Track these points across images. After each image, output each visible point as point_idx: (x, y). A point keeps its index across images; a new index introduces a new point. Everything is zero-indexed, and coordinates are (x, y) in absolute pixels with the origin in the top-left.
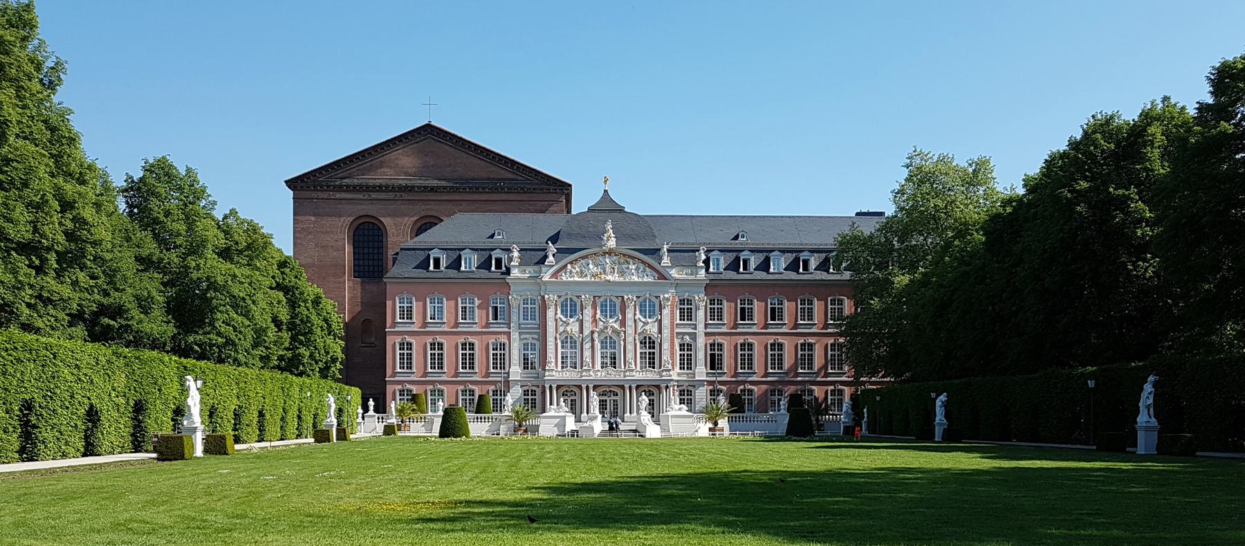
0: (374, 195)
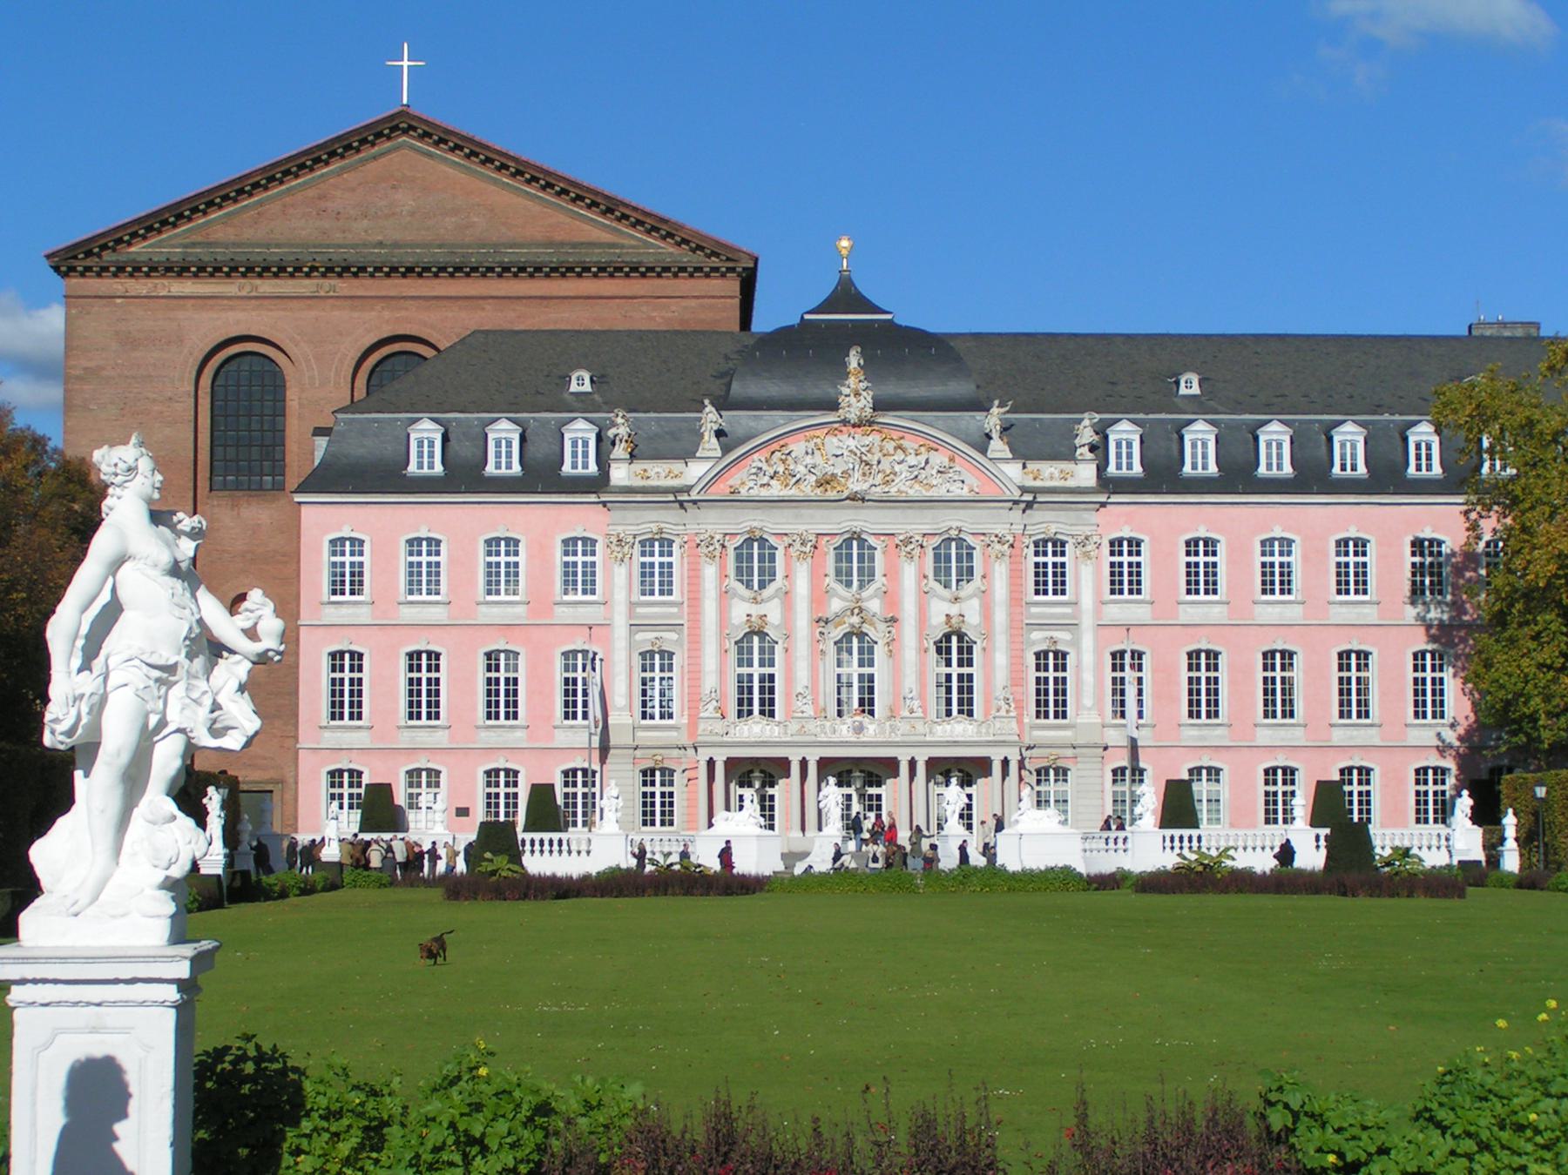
0: (267, 286)
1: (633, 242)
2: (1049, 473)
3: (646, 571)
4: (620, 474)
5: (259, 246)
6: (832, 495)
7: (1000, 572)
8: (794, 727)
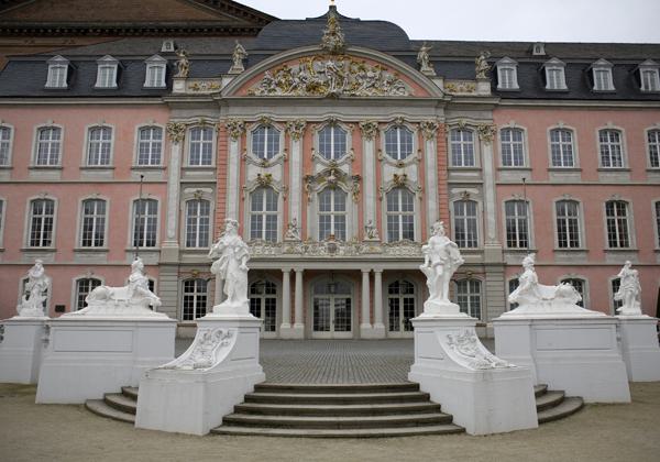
2: (460, 88)
3: (195, 148)
6: (317, 95)
7: (431, 148)
8: (286, 248)
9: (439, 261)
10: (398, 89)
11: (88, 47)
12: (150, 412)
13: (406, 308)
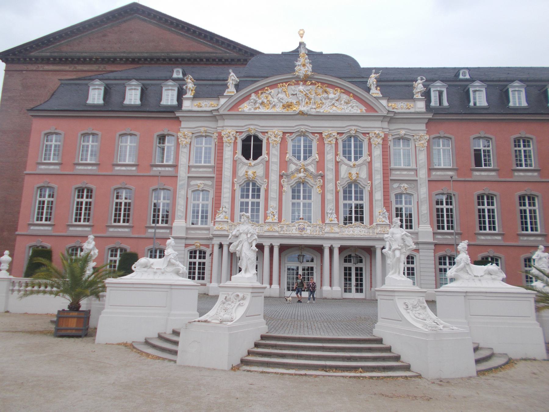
1: (220, 52)
2: (400, 106)
4: (187, 105)
5: (79, 52)
6: (290, 112)
7: (377, 152)
9: (397, 247)
10: (353, 107)
11: (120, 70)
12: (189, 351)
13: (357, 275)
